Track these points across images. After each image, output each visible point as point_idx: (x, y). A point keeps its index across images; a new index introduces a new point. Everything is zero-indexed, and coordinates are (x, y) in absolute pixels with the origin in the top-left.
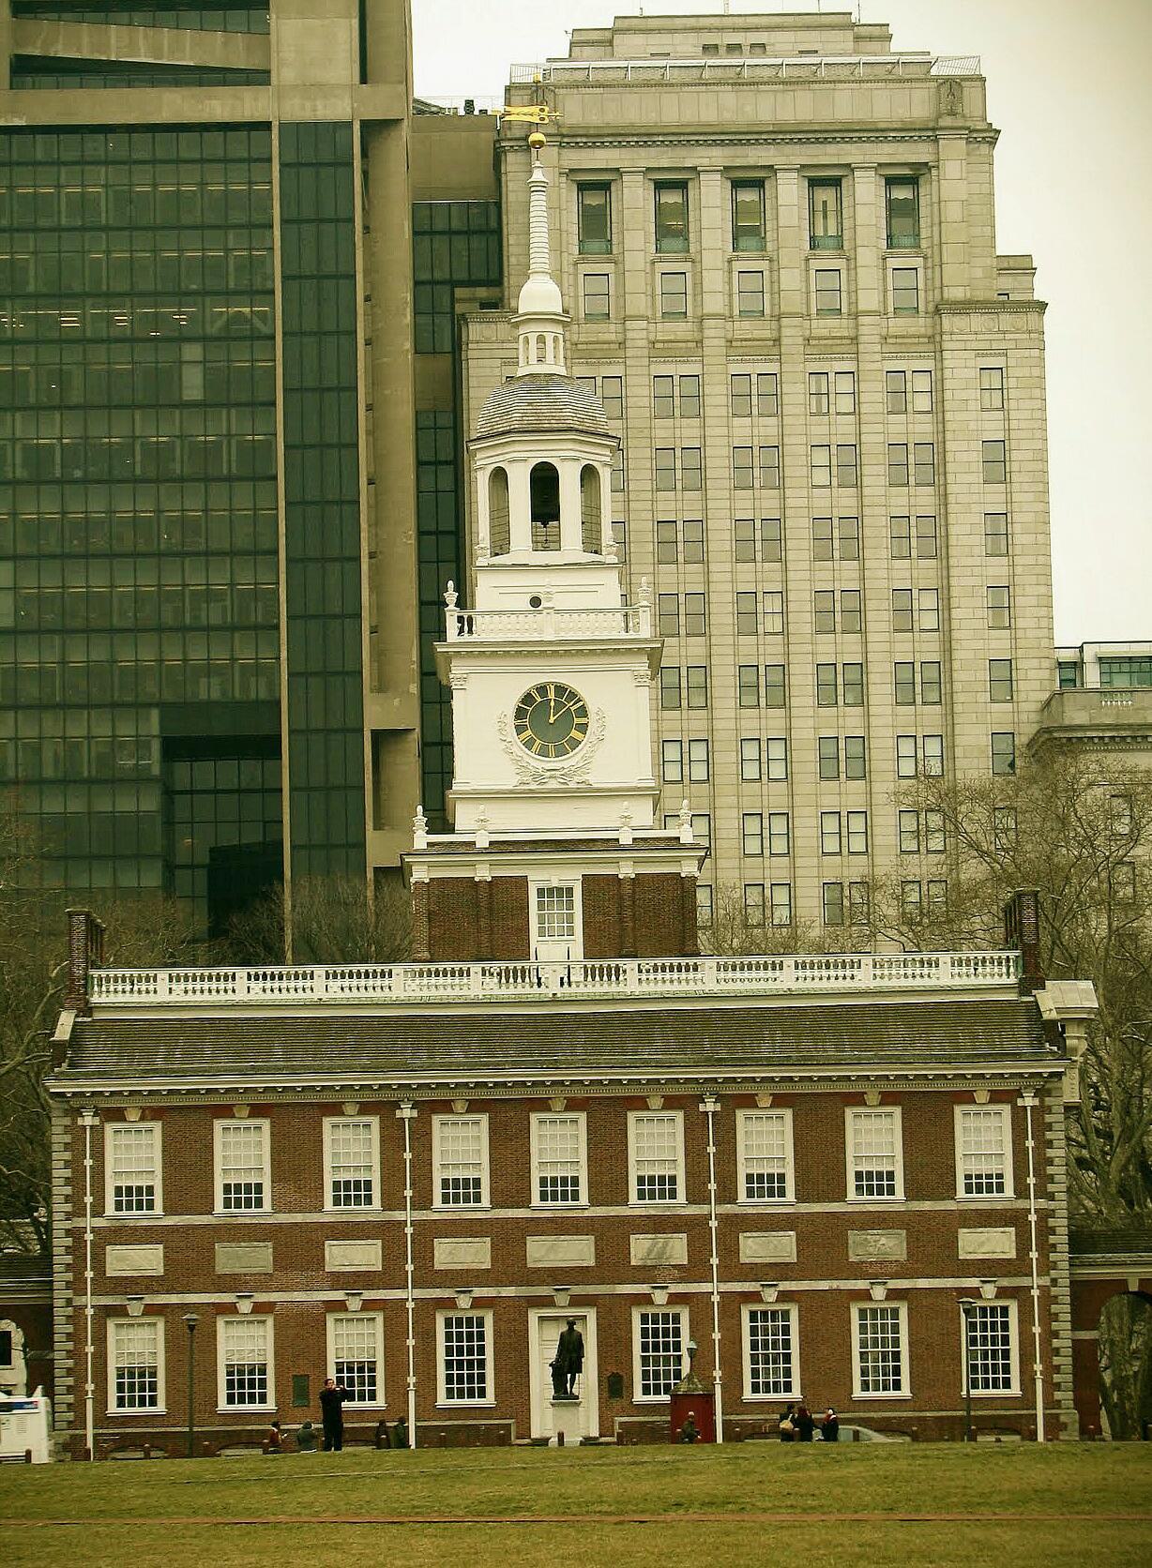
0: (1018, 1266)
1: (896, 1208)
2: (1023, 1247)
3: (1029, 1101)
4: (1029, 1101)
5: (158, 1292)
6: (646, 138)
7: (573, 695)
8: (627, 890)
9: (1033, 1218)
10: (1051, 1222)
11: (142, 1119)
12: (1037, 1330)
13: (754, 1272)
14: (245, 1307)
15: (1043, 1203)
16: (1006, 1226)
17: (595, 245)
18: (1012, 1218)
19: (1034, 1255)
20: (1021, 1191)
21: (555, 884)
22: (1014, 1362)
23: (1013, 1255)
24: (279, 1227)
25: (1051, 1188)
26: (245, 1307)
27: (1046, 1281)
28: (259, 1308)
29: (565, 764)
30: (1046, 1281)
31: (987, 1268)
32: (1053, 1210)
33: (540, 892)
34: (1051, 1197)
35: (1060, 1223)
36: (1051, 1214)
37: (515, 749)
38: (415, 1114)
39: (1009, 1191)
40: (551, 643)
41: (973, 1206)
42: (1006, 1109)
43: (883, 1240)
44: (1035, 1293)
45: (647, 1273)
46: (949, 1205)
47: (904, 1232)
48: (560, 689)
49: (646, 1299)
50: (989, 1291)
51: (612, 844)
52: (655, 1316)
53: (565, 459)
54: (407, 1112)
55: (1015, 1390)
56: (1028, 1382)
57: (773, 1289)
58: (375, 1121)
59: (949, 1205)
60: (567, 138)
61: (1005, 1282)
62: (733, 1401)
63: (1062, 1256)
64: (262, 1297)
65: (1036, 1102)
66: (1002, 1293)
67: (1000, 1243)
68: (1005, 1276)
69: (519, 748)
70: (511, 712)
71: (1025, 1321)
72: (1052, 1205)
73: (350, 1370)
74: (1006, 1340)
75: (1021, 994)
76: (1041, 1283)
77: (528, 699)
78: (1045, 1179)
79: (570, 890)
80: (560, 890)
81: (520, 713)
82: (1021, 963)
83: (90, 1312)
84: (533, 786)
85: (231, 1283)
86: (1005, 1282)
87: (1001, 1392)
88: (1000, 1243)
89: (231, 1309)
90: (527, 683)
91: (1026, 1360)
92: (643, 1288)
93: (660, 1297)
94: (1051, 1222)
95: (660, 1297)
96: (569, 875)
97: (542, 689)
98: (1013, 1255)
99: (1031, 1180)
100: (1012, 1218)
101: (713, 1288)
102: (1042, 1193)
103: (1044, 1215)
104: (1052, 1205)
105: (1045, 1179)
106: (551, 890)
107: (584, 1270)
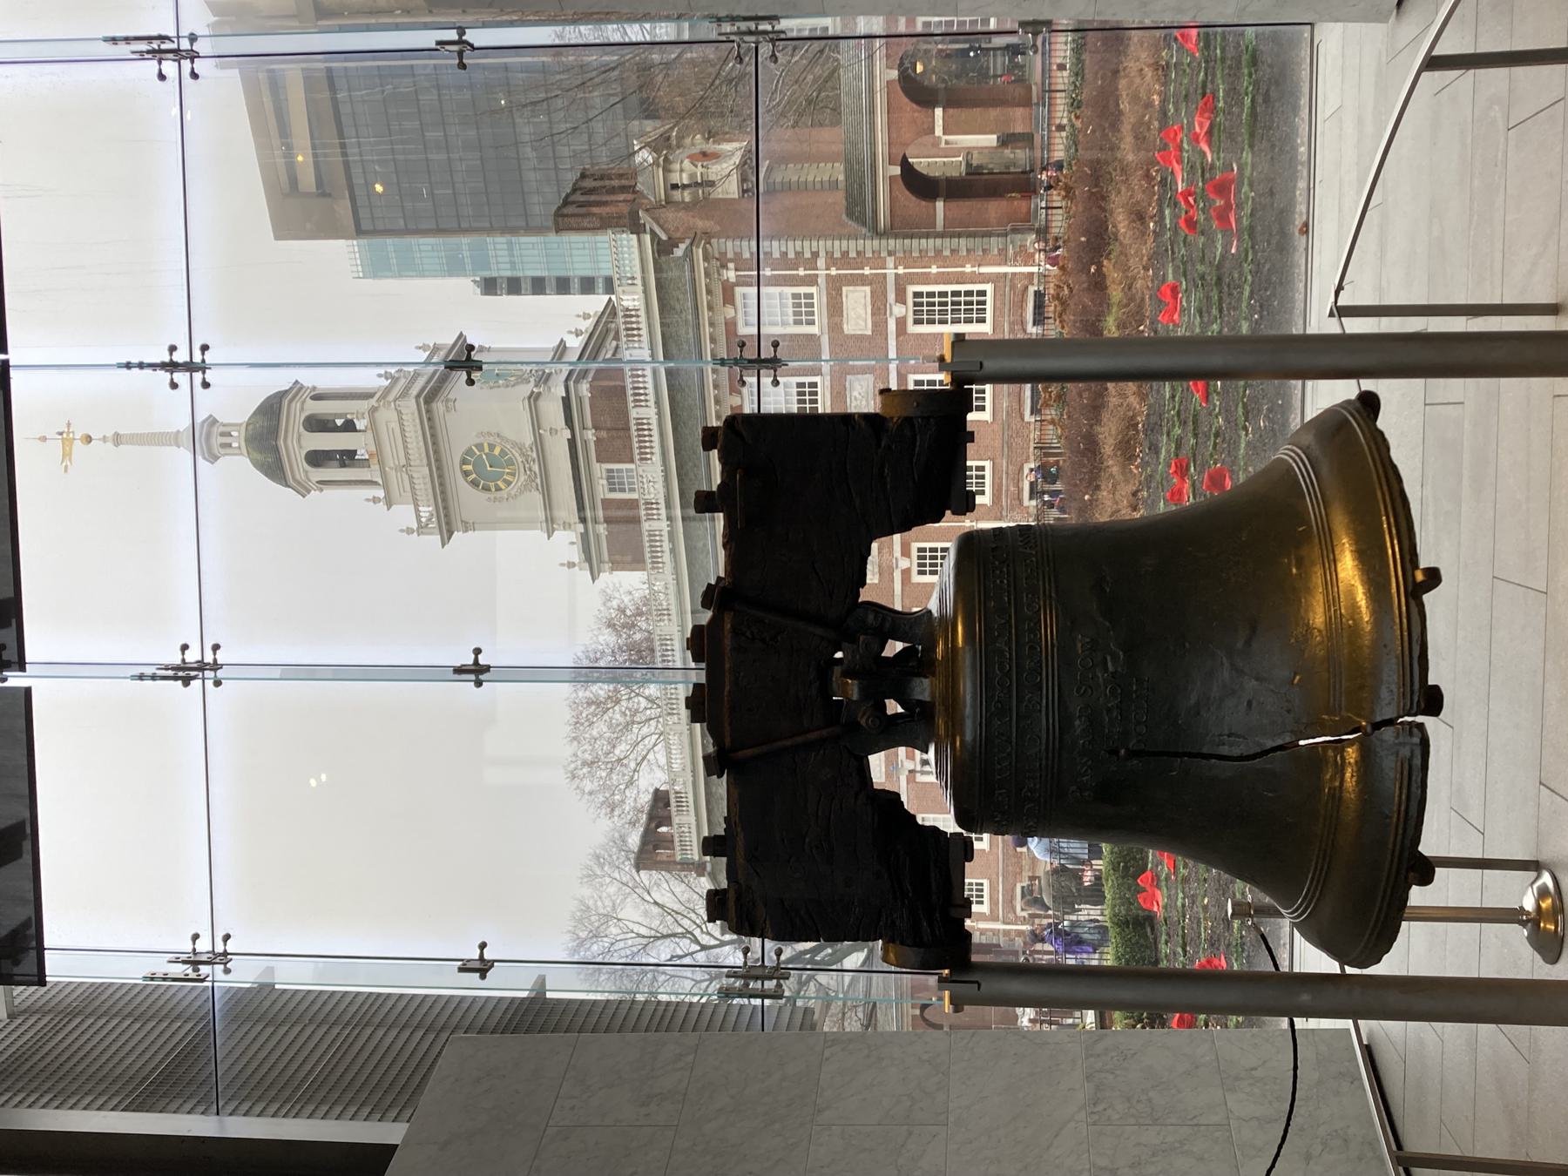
0: (878, 284)
1: (828, 383)
2: (862, 280)
3: (731, 275)
4: (731, 275)
7: (469, 452)
8: (604, 434)
9: (833, 272)
10: (837, 255)
12: (934, 270)
15: (821, 262)
16: (841, 295)
18: (835, 288)
19: (867, 271)
20: (812, 281)
21: (605, 482)
22: (963, 288)
23: (868, 289)
25: (808, 255)
27: (890, 261)
29: (520, 460)
30: (890, 261)
31: (879, 309)
32: (827, 253)
33: (611, 490)
34: (815, 255)
35: (837, 247)
36: (829, 255)
37: (513, 493)
39: (813, 290)
40: (431, 470)
41: (825, 321)
42: (739, 291)
43: (855, 394)
44: (901, 270)
46: (825, 340)
47: (848, 377)
48: (464, 462)
49: (906, 573)
50: (899, 310)
51: (572, 443)
52: (920, 565)
53: (300, 447)
55: (989, 288)
56: (985, 279)
59: (825, 340)
61: (891, 296)
63: (870, 245)
65: (731, 265)
66: (901, 299)
67: (857, 301)
68: (886, 297)
69: (512, 489)
70: (486, 495)
71: (926, 279)
72: (822, 254)
74: (943, 294)
75: (645, 232)
76: (892, 265)
77: (474, 484)
78: (799, 259)
79: (609, 471)
80: (608, 478)
81: (486, 489)
82: (618, 229)
84: (538, 481)
86: (891, 296)
87: (989, 298)
88: (857, 301)
90: (462, 484)
91: (961, 278)
93: (904, 563)
94: (837, 255)
95: (904, 563)
96: (599, 469)
97: (466, 474)
98: (868, 289)
99: (801, 272)
100: (835, 288)
102: (812, 263)
103: (832, 261)
104: (822, 254)
105: (799, 259)
106: (609, 484)
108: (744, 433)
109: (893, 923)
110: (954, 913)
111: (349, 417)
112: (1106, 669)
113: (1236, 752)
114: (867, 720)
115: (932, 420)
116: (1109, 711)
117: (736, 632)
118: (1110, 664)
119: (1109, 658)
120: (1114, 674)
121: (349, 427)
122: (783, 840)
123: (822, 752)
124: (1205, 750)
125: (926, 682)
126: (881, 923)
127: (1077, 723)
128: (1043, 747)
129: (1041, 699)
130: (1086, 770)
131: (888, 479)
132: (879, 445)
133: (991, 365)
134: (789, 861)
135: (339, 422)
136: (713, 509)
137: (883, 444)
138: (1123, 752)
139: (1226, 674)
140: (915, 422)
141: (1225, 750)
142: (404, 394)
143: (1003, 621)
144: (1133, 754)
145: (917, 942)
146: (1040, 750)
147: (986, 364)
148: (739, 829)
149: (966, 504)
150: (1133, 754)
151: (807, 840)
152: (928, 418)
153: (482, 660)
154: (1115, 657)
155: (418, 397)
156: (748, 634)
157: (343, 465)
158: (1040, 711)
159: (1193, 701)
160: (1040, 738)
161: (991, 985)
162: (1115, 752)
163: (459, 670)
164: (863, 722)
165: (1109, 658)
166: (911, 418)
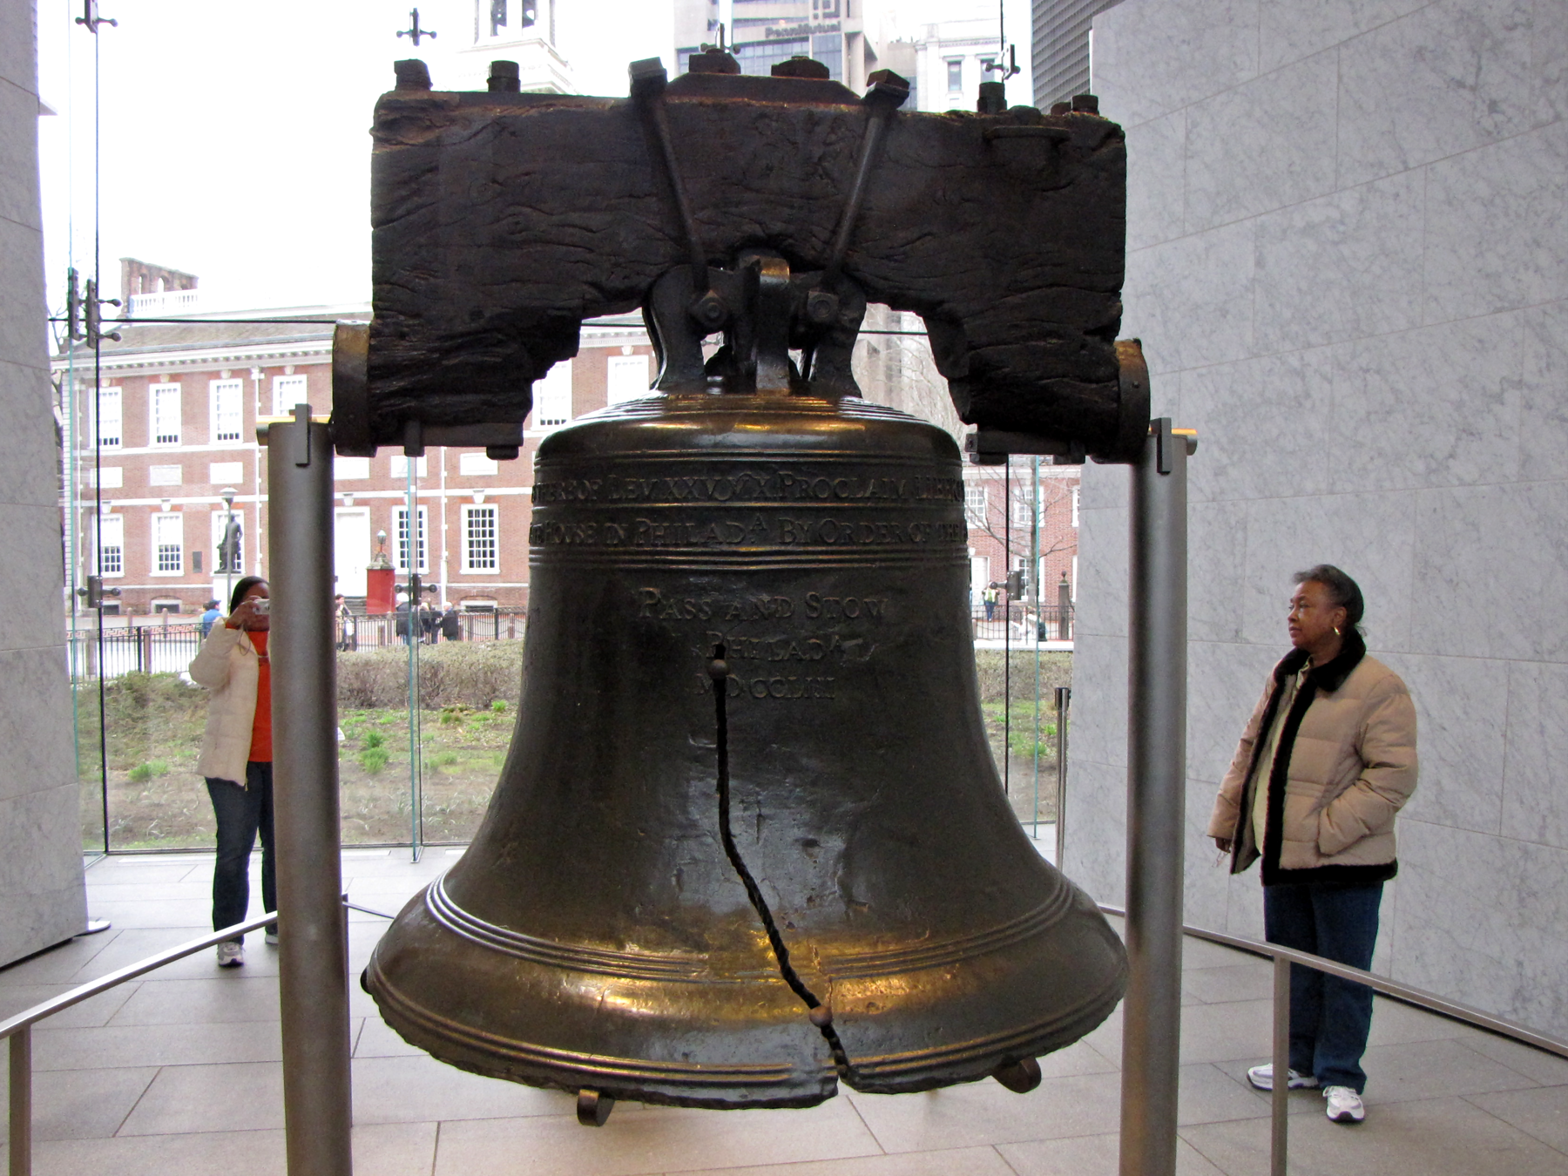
5: (119, 498)
6: (975, 42)
11: (111, 385)
13: (472, 482)
14: (166, 507)
17: (955, 87)
24: (185, 455)
26: (166, 507)
28: (175, 508)
38: (262, 376)
45: (399, 484)
54: (256, 375)
57: (480, 494)
58: (239, 381)
60: (942, 44)
62: (454, 575)
64: (175, 501)
73: (167, 550)
83: (80, 511)
85: (159, 492)
89: (158, 509)
92: (398, 494)
101: (443, 494)
107: (361, 481)
108: (1104, 150)
109: (403, 336)
110: (412, 430)
111: (536, 22)
112: (844, 637)
113: (735, 828)
114: (712, 300)
115: (1115, 405)
116: (787, 643)
117: (839, 119)
118: (854, 642)
119: (860, 641)
120: (838, 648)
121: (527, 22)
122: (527, 174)
123: (660, 235)
124: (732, 783)
125: (784, 386)
126: (402, 318)
127: (766, 598)
128: (725, 548)
129: (799, 544)
130: (689, 612)
131: (1042, 343)
132: (1087, 333)
133: (1159, 486)
134: (494, 181)
135: (530, 14)
136: (982, 103)
137: (1089, 338)
138: (720, 664)
139: (849, 805)
140: (1114, 382)
141: (736, 811)
142: (554, 71)
143: (901, 490)
144: (720, 683)
145: (377, 371)
146: (721, 543)
147: (1166, 479)
148: (543, 110)
149: (990, 454)
150: (720, 683)
151: (528, 210)
152: (1118, 398)
153: (422, 38)
154: (864, 648)
155: (553, 84)
156: (833, 137)
157: (494, 15)
158: (784, 543)
159: (804, 761)
160: (737, 544)
161: (301, 483)
162: (720, 652)
163: (415, 15)
164: (711, 294)
165: (860, 641)
166: (1117, 378)
